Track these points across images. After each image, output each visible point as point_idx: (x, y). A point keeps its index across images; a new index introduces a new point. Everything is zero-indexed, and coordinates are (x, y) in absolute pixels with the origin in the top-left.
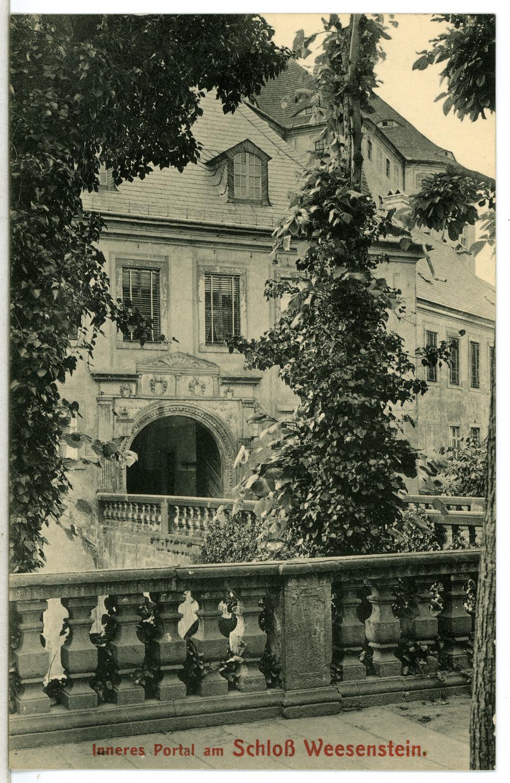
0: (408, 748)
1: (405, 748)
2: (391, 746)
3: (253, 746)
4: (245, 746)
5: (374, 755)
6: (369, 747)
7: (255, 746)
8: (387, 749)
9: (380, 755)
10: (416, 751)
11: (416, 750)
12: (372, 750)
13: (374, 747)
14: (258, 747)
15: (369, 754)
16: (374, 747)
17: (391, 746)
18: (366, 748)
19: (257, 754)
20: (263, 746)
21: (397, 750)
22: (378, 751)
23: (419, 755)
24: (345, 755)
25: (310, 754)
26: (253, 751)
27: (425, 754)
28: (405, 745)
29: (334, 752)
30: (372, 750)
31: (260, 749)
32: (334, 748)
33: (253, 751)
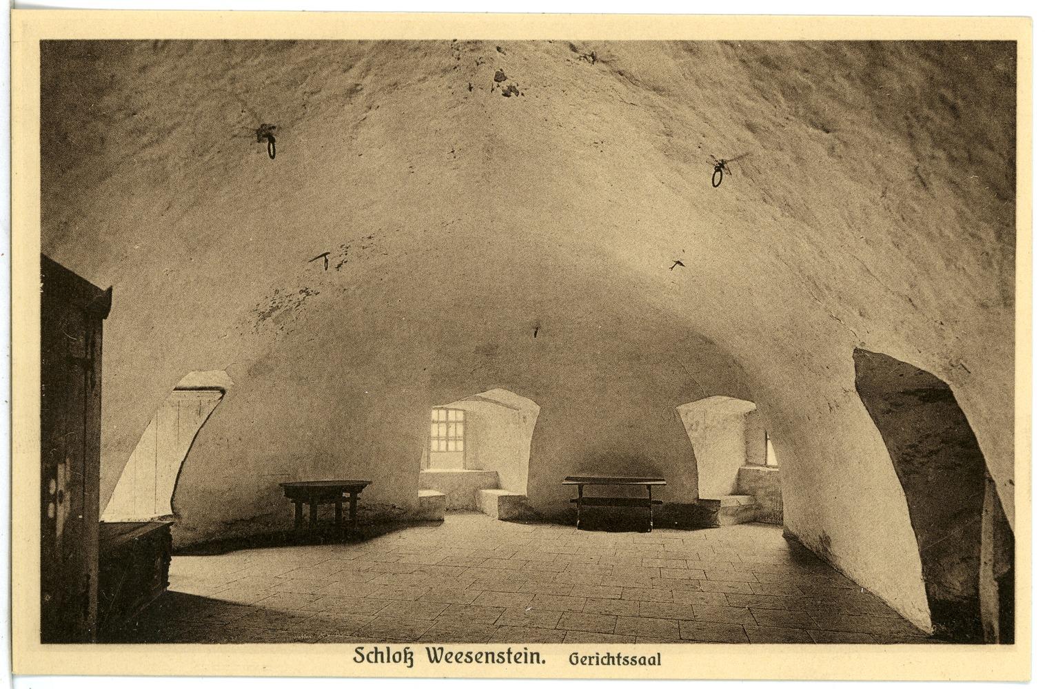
0: (526, 654)
1: (523, 655)
2: (509, 653)
3: (372, 653)
4: (365, 652)
5: (493, 662)
6: (487, 654)
7: (374, 650)
8: (505, 656)
9: (498, 661)
10: (535, 657)
11: (535, 656)
12: (490, 656)
13: (493, 654)
14: (377, 653)
15: (487, 662)
16: (493, 654)
17: (509, 653)
18: (484, 655)
19: (376, 661)
20: (382, 653)
21: (515, 656)
22: (496, 657)
23: (538, 662)
24: (464, 663)
25: (432, 662)
26: (372, 657)
27: (544, 662)
28: (523, 651)
29: (453, 659)
30: (490, 656)
31: (379, 656)
32: (454, 655)
33: (372, 657)
